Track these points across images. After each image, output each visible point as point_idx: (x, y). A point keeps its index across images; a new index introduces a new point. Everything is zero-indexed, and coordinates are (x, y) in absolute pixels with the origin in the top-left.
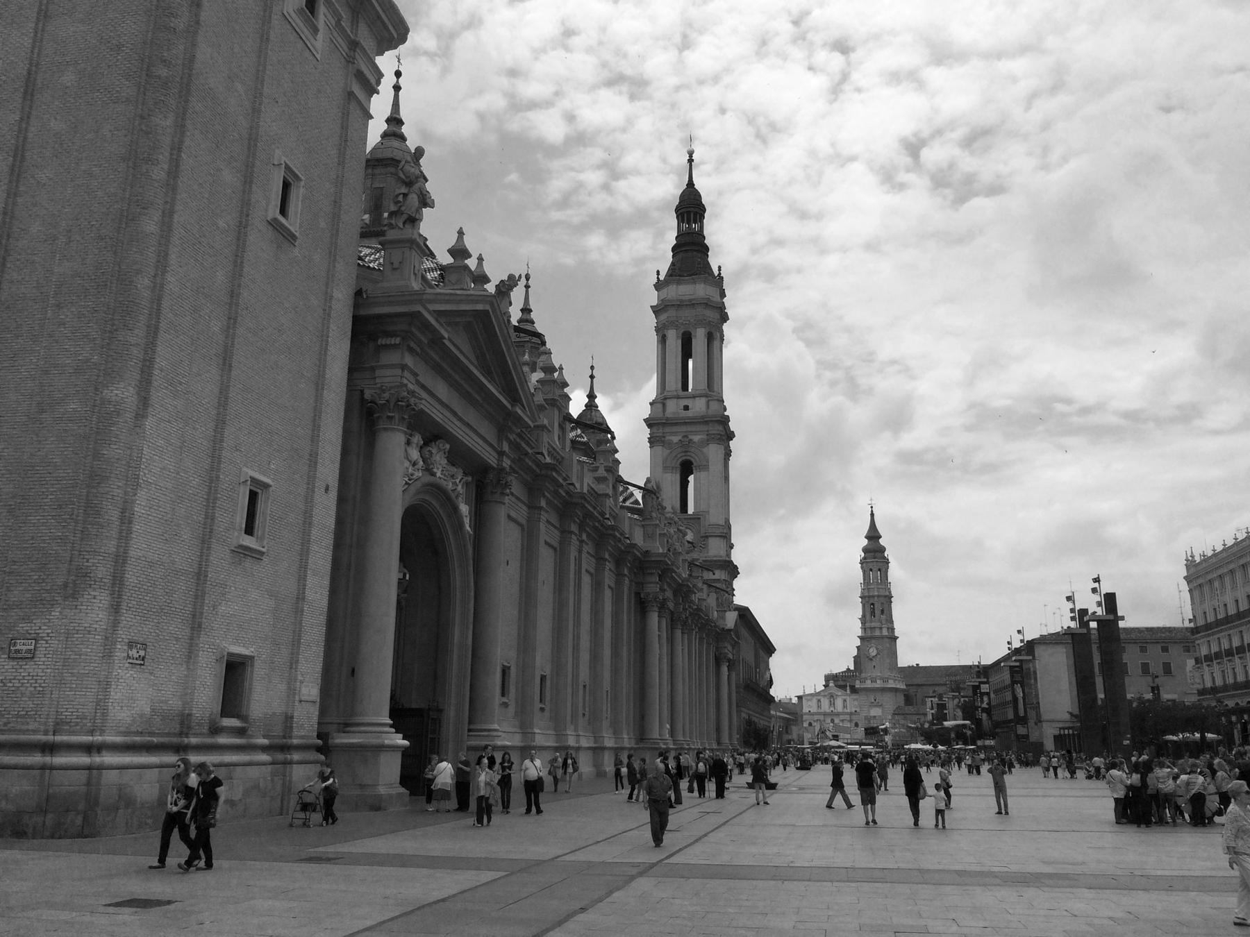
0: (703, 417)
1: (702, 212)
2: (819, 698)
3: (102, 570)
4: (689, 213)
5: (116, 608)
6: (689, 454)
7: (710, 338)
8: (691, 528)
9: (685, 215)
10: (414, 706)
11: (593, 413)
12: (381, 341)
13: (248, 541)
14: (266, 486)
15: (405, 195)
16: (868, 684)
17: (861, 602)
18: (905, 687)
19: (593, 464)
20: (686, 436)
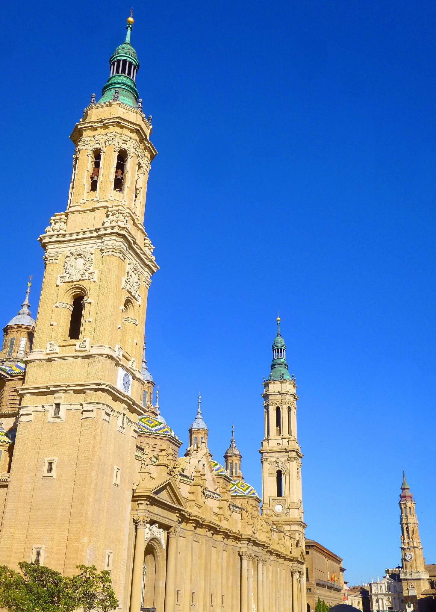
0: (285, 449)
1: (285, 349)
2: (381, 584)
4: (278, 349)
6: (280, 467)
7: (289, 409)
8: (281, 504)
9: (277, 350)
10: (148, 607)
11: (234, 449)
12: (139, 502)
14: (111, 553)
16: (408, 576)
17: (401, 527)
18: (429, 578)
19: (219, 498)
20: (277, 458)
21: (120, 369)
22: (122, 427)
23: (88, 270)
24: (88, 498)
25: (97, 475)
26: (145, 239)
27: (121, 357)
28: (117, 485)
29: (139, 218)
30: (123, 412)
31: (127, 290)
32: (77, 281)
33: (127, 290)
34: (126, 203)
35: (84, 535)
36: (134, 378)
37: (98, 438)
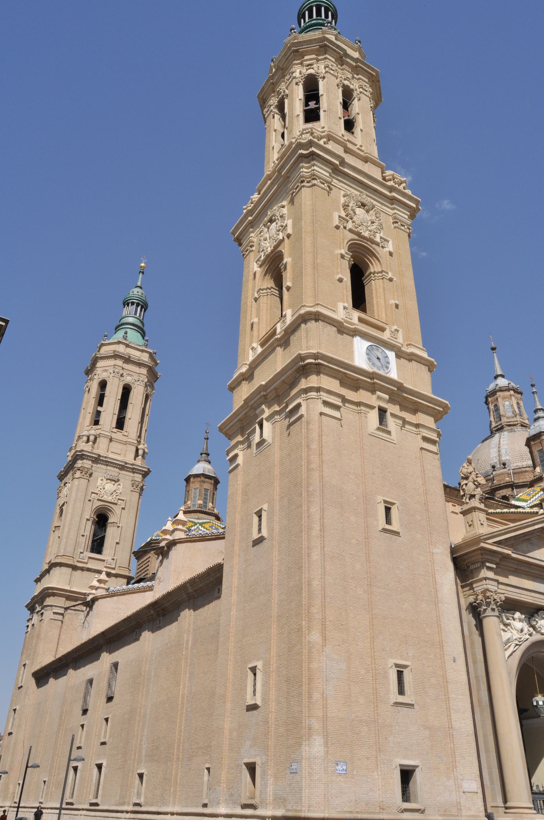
3: (316, 725)
5: (326, 744)
13: (401, 699)
14: (406, 667)
15: (466, 484)
21: (357, 340)
22: (378, 429)
23: (281, 227)
24: (309, 555)
25: (323, 510)
26: (383, 172)
27: (355, 320)
28: (397, 533)
29: (363, 148)
30: (376, 403)
31: (350, 231)
32: (272, 251)
33: (350, 231)
34: (326, 129)
35: (309, 629)
36: (400, 354)
37: (314, 446)
